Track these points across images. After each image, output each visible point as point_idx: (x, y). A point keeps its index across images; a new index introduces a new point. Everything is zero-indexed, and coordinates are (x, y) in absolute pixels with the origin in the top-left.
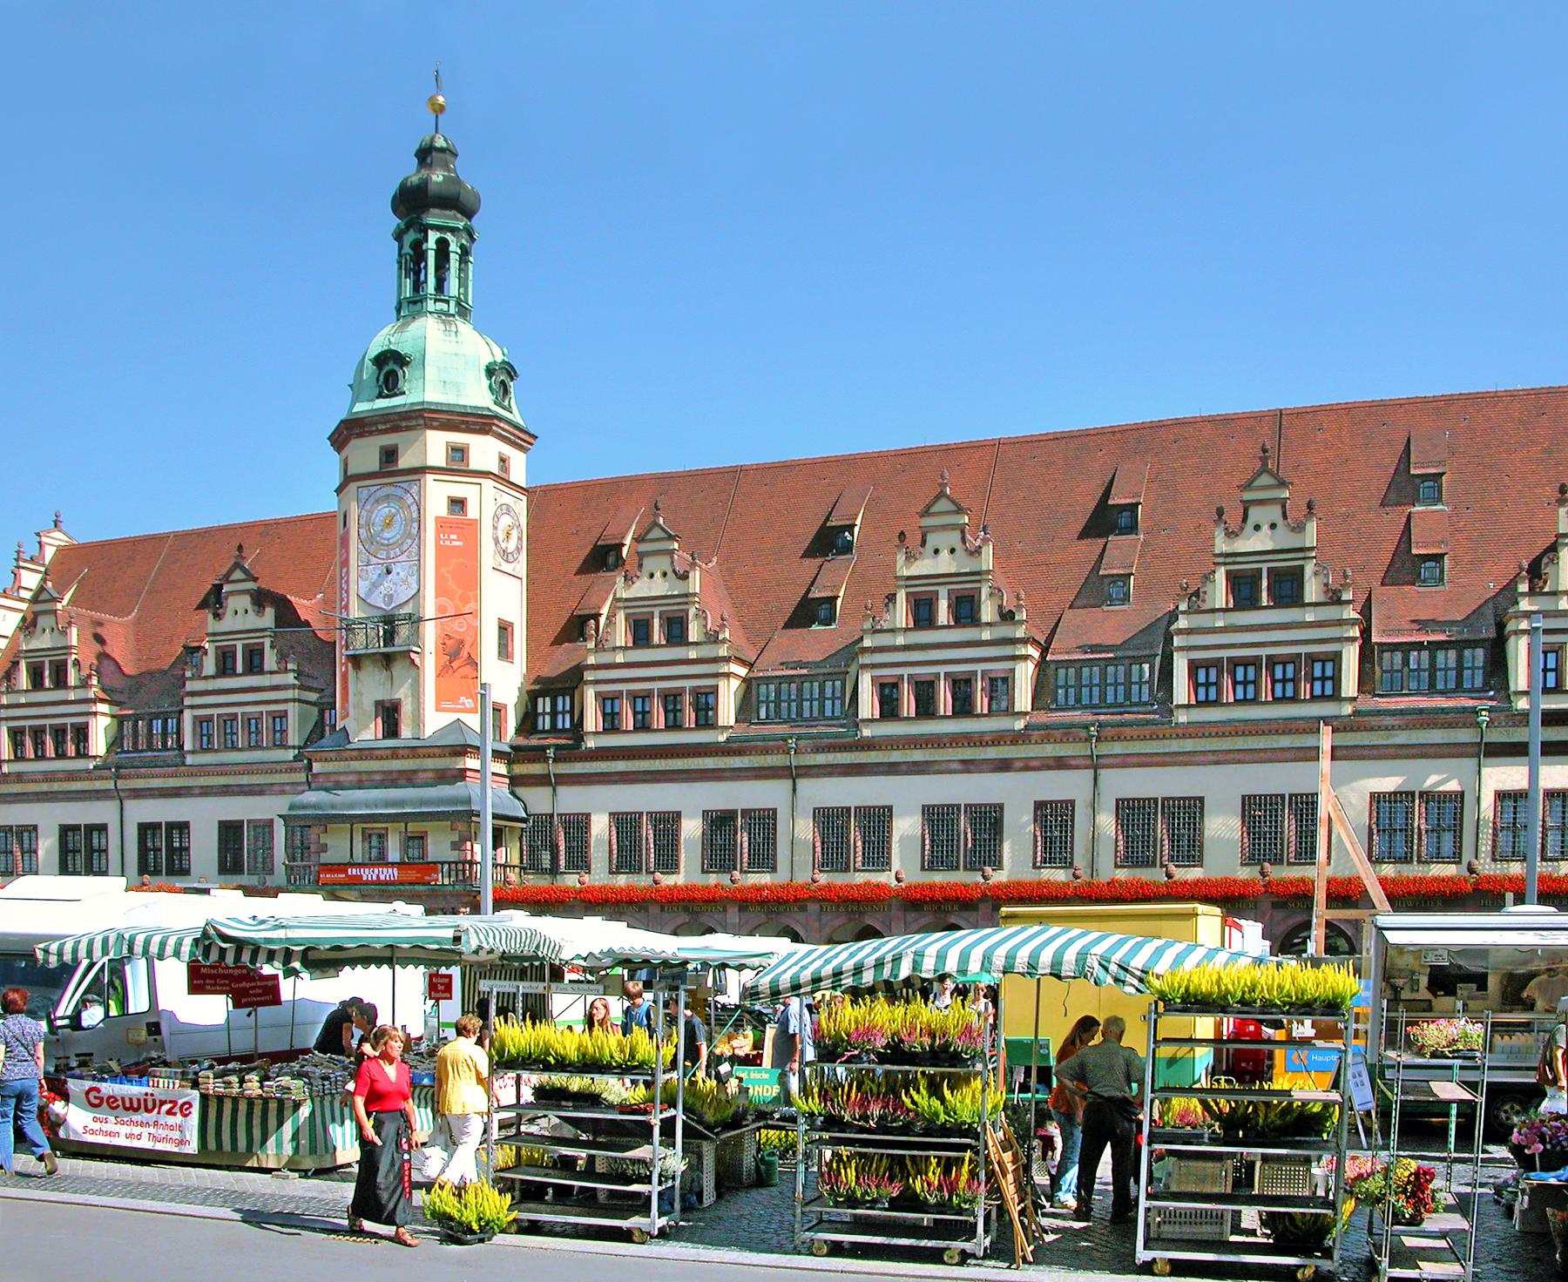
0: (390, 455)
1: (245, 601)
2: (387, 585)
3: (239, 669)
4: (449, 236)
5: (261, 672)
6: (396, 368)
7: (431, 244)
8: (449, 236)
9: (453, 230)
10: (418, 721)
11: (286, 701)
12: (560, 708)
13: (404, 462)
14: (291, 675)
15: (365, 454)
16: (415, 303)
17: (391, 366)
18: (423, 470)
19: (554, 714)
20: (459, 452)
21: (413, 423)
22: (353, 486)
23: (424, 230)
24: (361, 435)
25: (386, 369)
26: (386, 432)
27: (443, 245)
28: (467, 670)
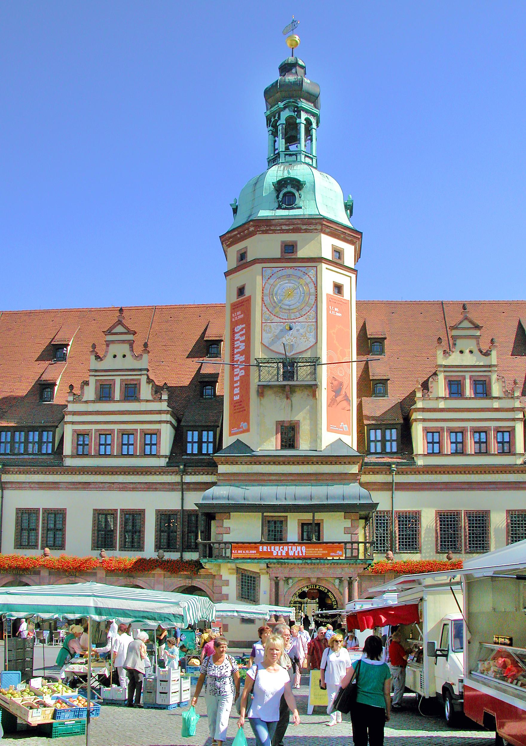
2: (287, 339)
3: (117, 395)
5: (137, 399)
6: (294, 191)
9: (314, 115)
10: (316, 436)
13: (301, 253)
14: (166, 404)
16: (290, 155)
18: (321, 260)
20: (338, 253)
21: (313, 227)
22: (258, 267)
23: (298, 110)
24: (265, 232)
26: (288, 231)
27: (309, 123)
28: (344, 403)
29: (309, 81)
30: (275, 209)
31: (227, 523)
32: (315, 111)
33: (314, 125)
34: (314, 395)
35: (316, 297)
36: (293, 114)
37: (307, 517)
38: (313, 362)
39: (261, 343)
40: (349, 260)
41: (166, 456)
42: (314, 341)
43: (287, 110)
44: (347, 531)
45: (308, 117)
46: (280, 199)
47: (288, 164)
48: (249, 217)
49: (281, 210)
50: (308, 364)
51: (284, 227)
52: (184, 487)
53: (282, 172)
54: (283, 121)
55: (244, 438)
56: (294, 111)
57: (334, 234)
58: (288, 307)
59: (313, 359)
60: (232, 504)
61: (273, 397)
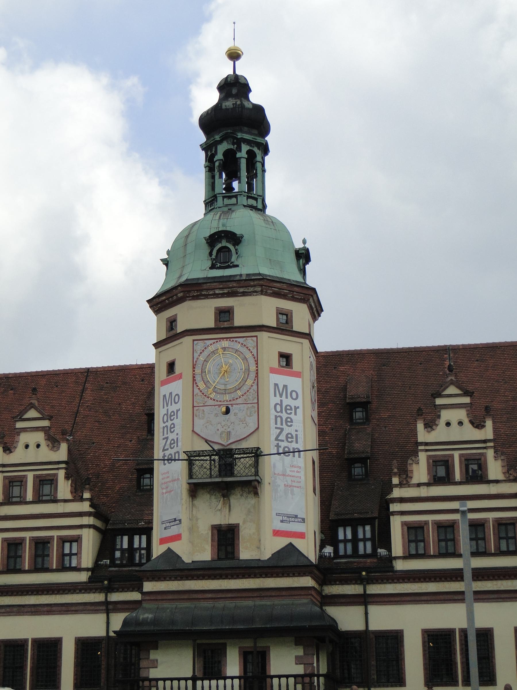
1: (40, 437)
3: (30, 497)
4: (255, 149)
5: (55, 501)
8: (255, 149)
11: (81, 527)
12: (361, 536)
15: (198, 313)
16: (230, 197)
17: (224, 243)
19: (355, 540)
21: (251, 289)
22: (188, 340)
25: (219, 246)
26: (223, 295)
27: (251, 155)
31: (153, 655)
32: (259, 140)
34: (256, 494)
35: (257, 373)
37: (248, 644)
38: (251, 453)
39: (193, 431)
41: (87, 570)
42: (257, 427)
44: (299, 660)
45: (251, 148)
47: (226, 209)
49: (215, 270)
50: (245, 456)
51: (217, 292)
52: (109, 608)
55: (177, 547)
57: (277, 295)
58: (222, 387)
59: (250, 450)
60: (158, 630)
61: (207, 496)
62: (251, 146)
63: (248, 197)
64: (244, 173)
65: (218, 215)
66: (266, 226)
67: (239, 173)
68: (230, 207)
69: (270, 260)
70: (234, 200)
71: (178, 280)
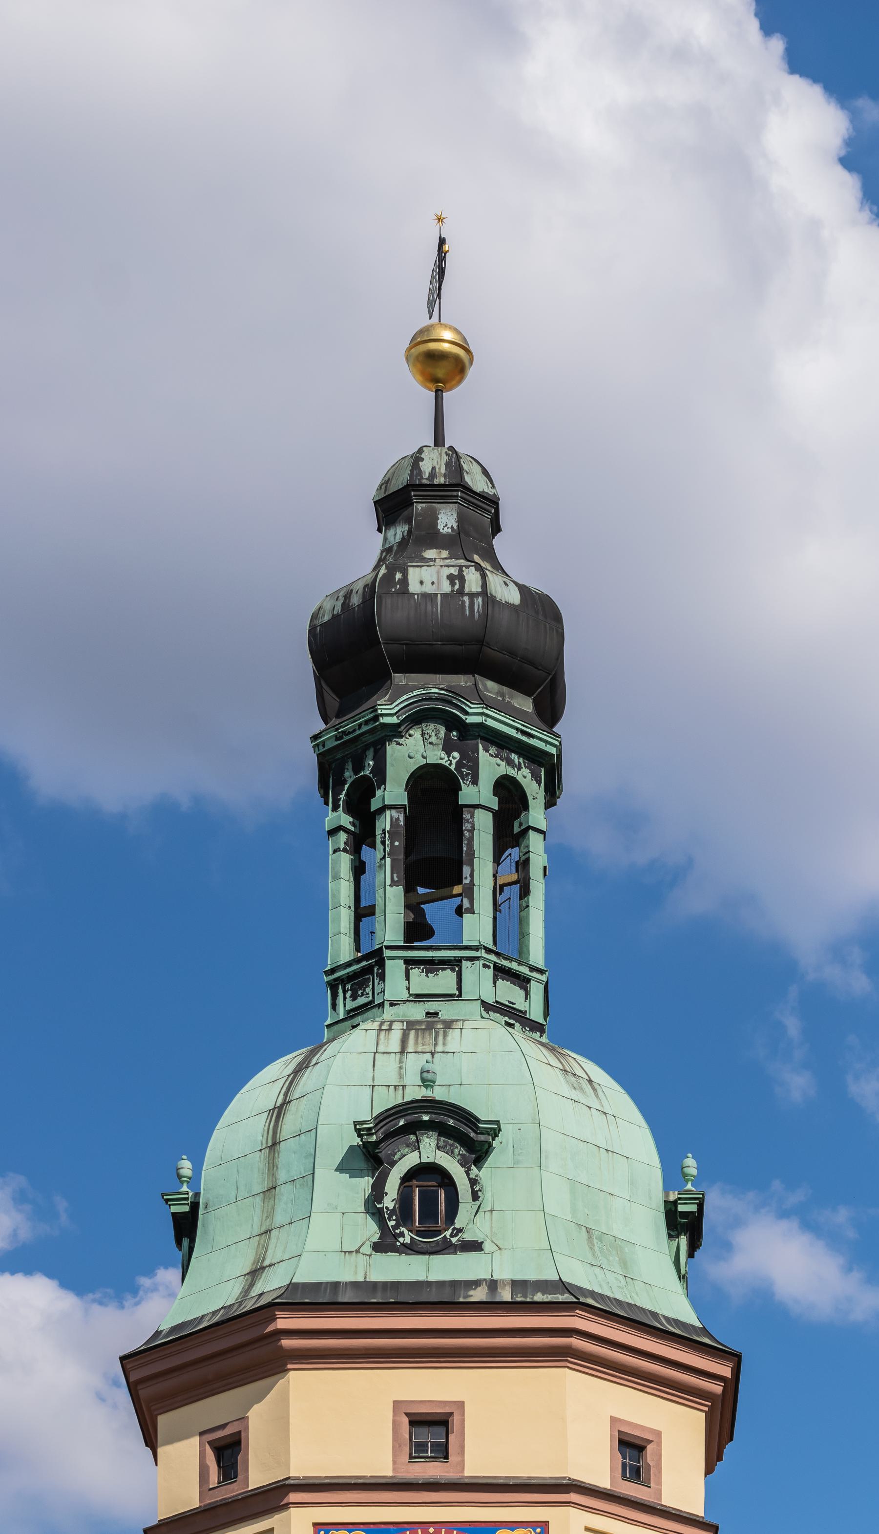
0: (431, 1430)
4: (524, 776)
7: (479, 793)
8: (524, 776)
16: (431, 966)
29: (513, 597)
30: (367, 1249)
32: (540, 740)
33: (537, 815)
36: (437, 756)
40: (682, 1481)
43: (416, 733)
45: (512, 772)
46: (389, 1202)
47: (417, 1012)
48: (255, 1273)
53: (394, 1060)
54: (394, 792)
56: (448, 748)
62: (510, 763)
63: (501, 972)
64: (482, 871)
65: (396, 1035)
66: (575, 1095)
67: (466, 870)
68: (432, 1006)
69: (588, 1230)
70: (445, 981)
71: (251, 1285)
